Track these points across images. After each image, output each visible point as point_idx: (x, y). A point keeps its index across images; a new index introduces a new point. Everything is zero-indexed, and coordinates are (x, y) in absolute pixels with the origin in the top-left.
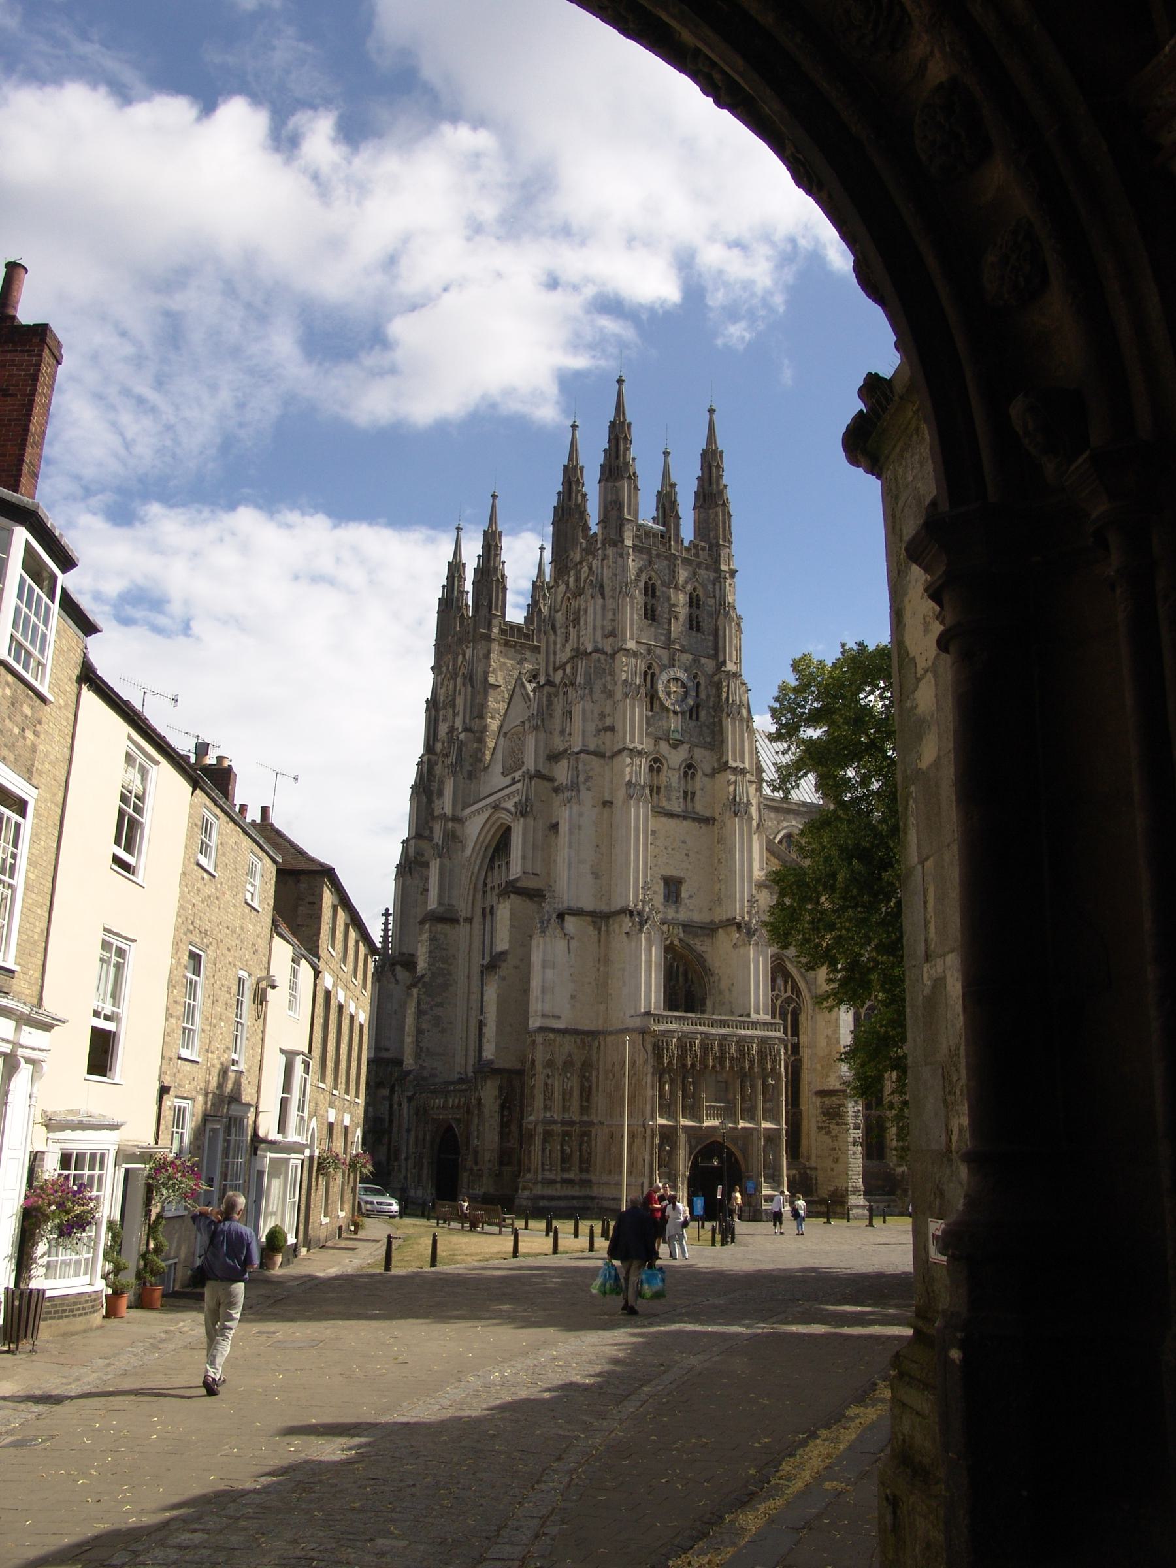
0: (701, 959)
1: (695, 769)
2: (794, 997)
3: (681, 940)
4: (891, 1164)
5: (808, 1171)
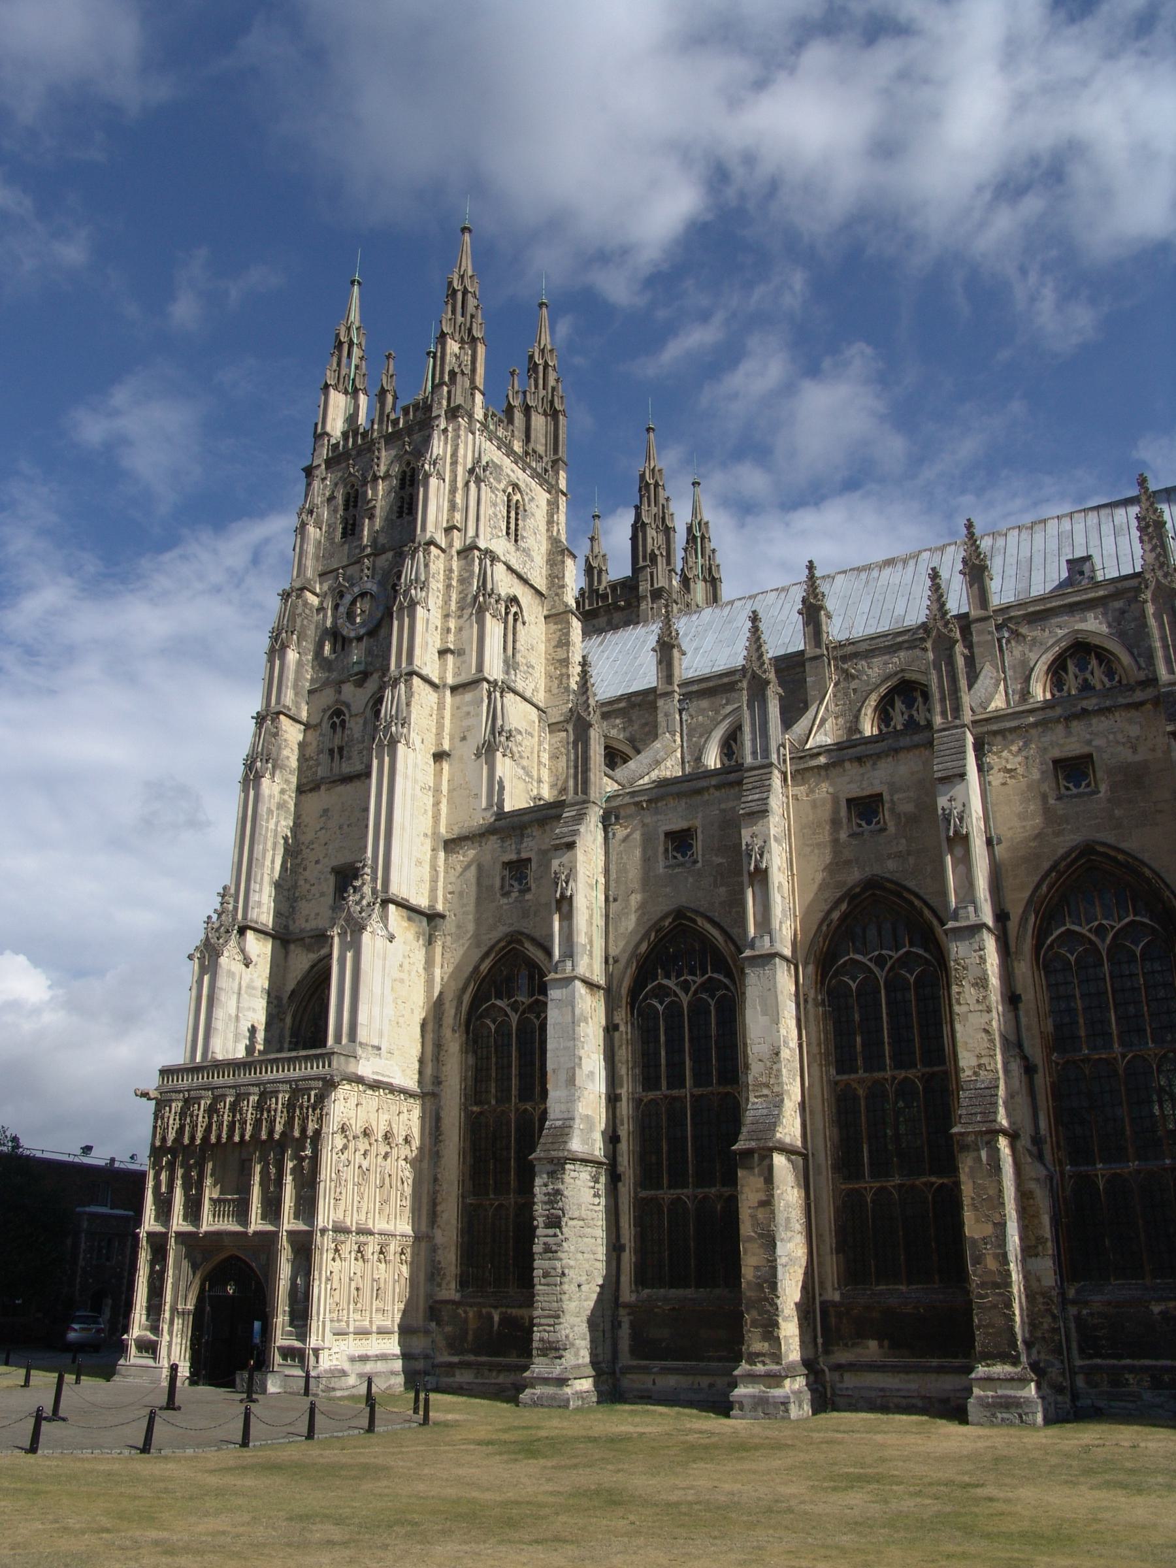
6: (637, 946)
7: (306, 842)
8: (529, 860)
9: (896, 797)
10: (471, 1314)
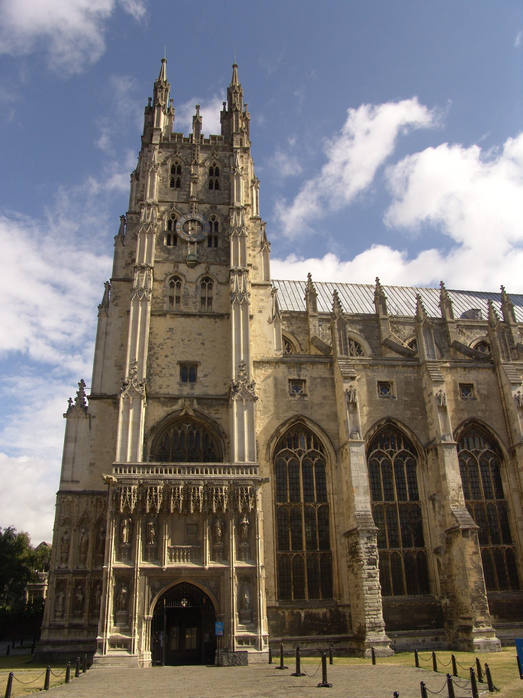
0: (214, 423)
1: (212, 281)
2: (318, 451)
3: (195, 411)
4: (437, 598)
5: (341, 609)
6: (369, 431)
7: (157, 344)
8: (305, 381)
9: (479, 387)
10: (287, 614)
